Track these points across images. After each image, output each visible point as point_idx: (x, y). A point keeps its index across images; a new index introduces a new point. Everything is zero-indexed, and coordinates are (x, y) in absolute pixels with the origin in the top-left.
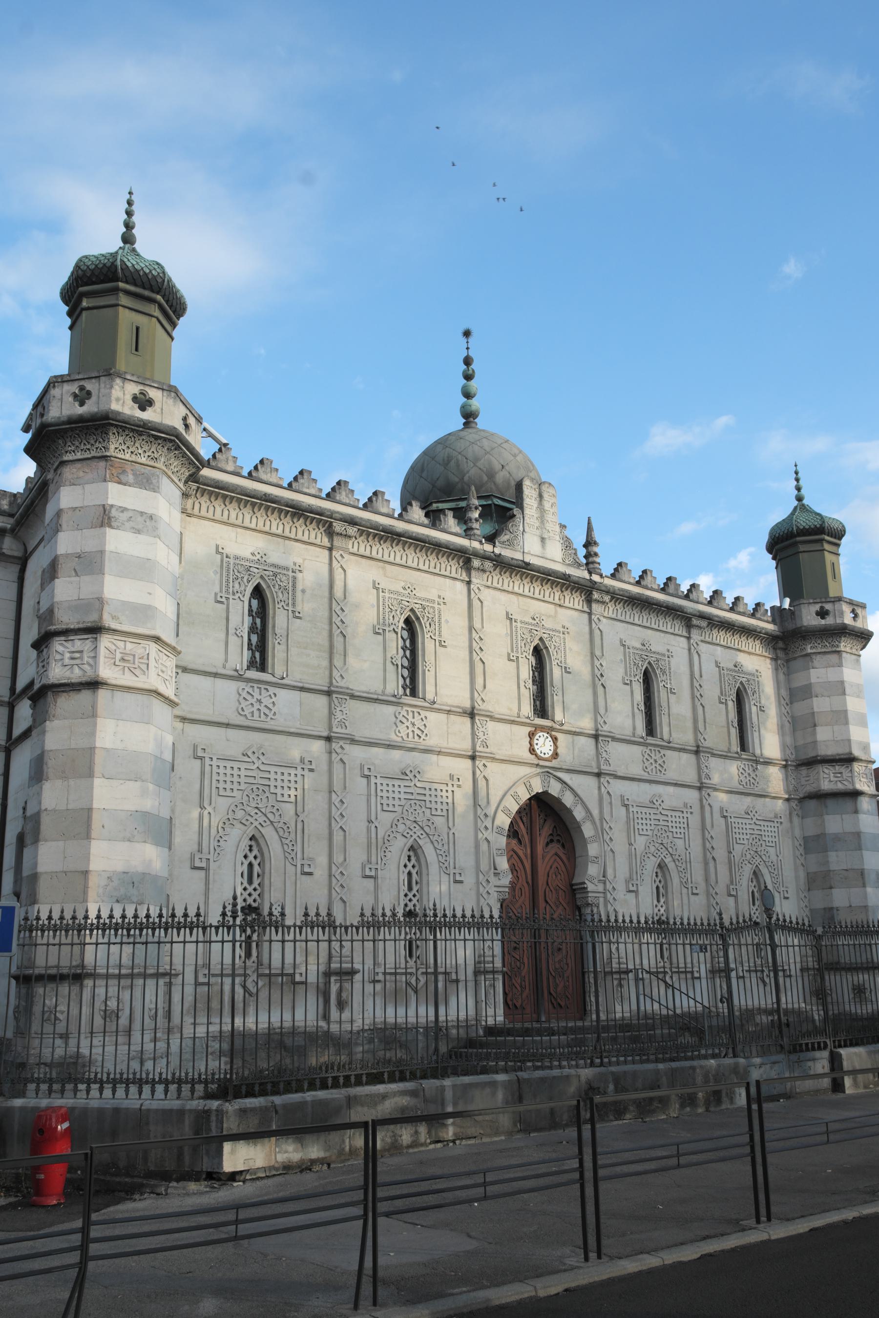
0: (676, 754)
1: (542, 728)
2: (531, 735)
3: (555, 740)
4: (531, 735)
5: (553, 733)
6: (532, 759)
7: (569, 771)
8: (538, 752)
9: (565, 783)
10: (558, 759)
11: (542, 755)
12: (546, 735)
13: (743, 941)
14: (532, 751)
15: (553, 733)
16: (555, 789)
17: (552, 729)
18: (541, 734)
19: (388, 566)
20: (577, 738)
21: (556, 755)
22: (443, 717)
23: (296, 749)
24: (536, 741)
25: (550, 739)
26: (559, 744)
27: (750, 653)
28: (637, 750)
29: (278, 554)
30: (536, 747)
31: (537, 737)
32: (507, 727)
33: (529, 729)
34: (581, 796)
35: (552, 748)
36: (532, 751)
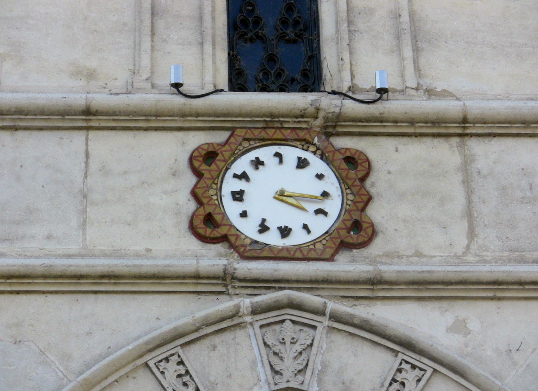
1: (272, 131)
3: (353, 170)
4: (207, 164)
6: (212, 258)
7: (426, 288)
8: (248, 229)
9: (409, 345)
10: (376, 248)
11: (272, 238)
12: (291, 154)
14: (208, 225)
15: (341, 143)
17: (334, 125)
18: (265, 153)
20: (487, 153)
21: (355, 231)
24: (230, 185)
25: (317, 164)
26: (377, 183)
30: (232, 209)
31: (242, 164)
32: (64, 149)
33: (197, 140)
35: (333, 207)
36: (208, 225)
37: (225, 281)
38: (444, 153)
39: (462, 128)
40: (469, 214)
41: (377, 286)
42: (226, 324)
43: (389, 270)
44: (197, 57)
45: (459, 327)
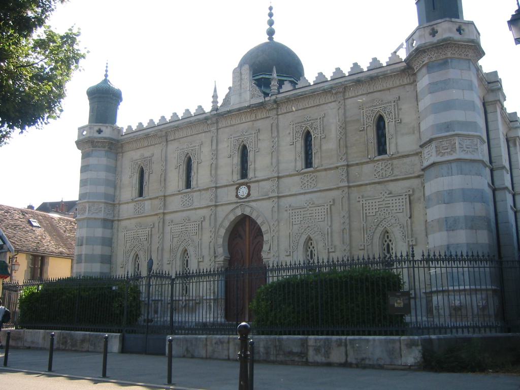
0: (324, 173)
2: (237, 189)
3: (249, 188)
5: (248, 185)
13: (164, 283)
14: (237, 196)
15: (248, 185)
16: (247, 212)
17: (247, 183)
19: (181, 140)
20: (261, 184)
21: (249, 195)
22: (198, 193)
23: (150, 220)
26: (251, 189)
27: (389, 89)
28: (297, 178)
29: (147, 153)
32: (226, 189)
33: (236, 186)
34: (261, 212)
36: (237, 196)
37: (237, 203)
38: (256, 184)
39: (258, 181)
40: (258, 191)
41: (249, 201)
42: (237, 207)
43: (251, 199)
44: (236, 177)
45: (257, 204)
